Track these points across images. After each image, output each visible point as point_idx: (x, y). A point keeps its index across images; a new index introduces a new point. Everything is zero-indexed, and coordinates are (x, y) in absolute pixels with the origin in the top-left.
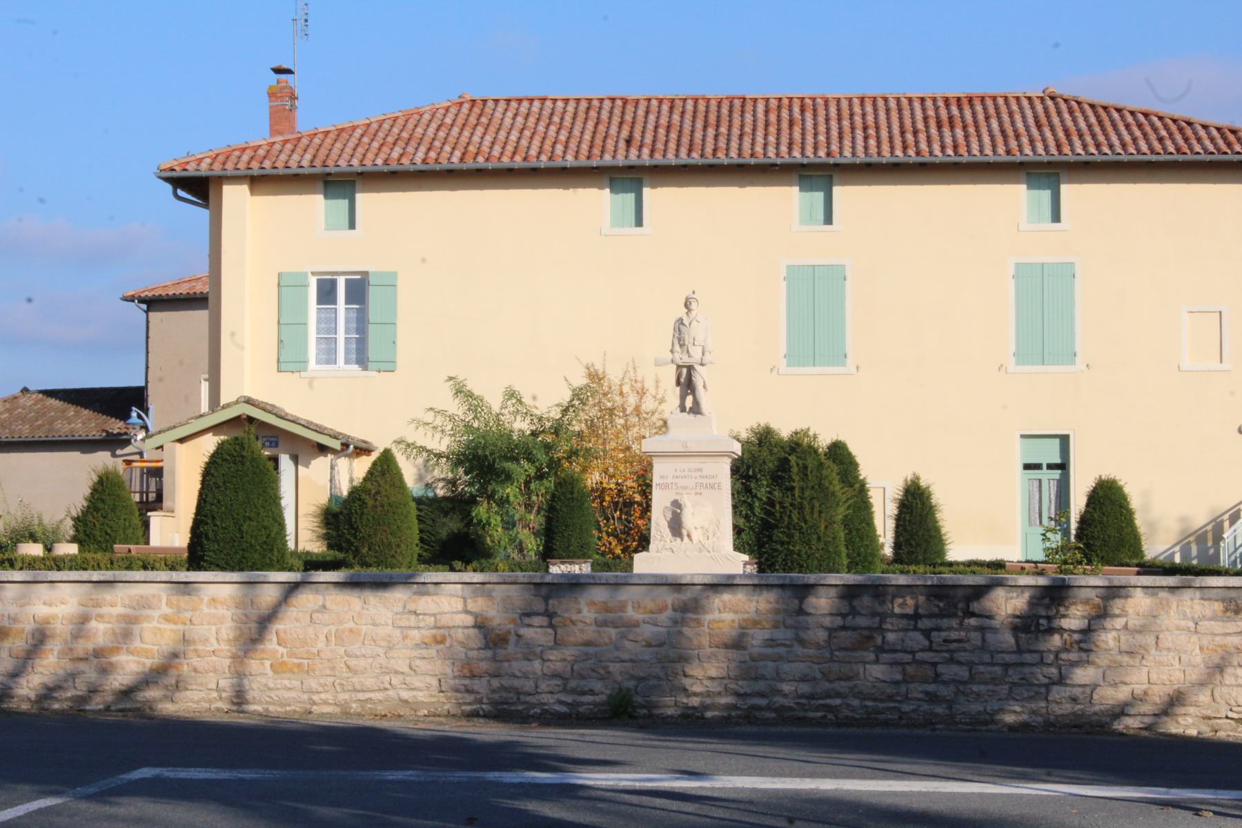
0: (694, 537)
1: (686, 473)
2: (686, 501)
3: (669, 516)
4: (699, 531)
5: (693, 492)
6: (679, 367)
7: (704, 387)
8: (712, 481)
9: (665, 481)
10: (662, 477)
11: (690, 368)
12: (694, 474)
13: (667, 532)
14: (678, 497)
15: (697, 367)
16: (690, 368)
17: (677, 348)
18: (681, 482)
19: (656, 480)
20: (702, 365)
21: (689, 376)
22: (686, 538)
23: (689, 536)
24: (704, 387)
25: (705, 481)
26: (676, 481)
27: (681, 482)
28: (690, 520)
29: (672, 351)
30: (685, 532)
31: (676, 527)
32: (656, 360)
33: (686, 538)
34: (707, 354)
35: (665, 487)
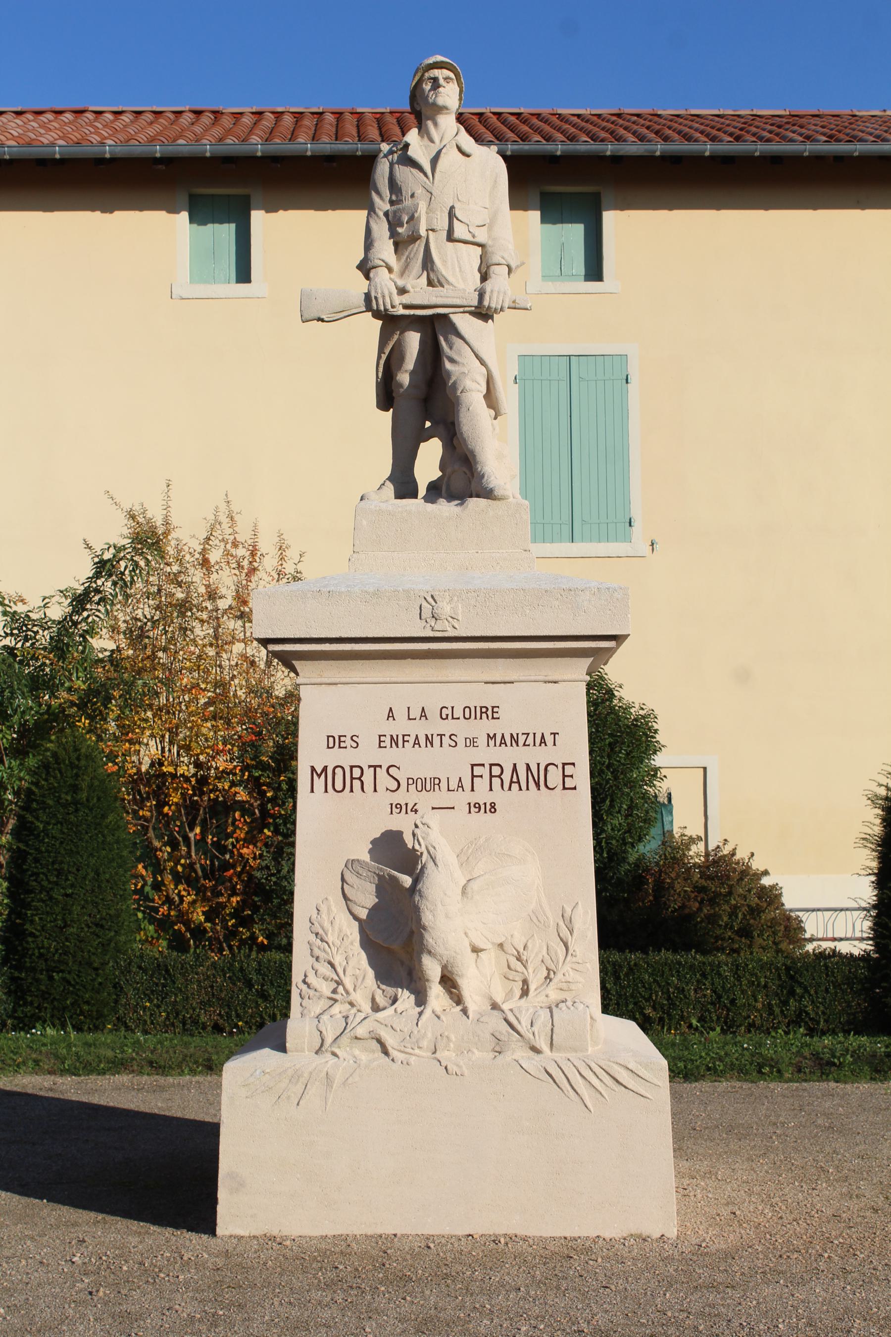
0: (469, 986)
1: (435, 726)
2: (440, 835)
3: (366, 898)
4: (489, 957)
5: (462, 799)
6: (392, 324)
7: (490, 398)
8: (537, 756)
9: (345, 757)
10: (335, 742)
11: (435, 327)
12: (463, 729)
13: (358, 965)
14: (402, 823)
15: (464, 323)
16: (435, 327)
17: (385, 249)
18: (413, 762)
19: (310, 753)
20: (483, 313)
21: (433, 358)
22: (436, 993)
23: (448, 981)
24: (490, 398)
25: (507, 756)
26: (388, 756)
27: (413, 762)
28: (453, 920)
29: (366, 268)
30: (432, 969)
31: (397, 944)
32: (305, 298)
33: (436, 993)
34: (499, 273)
35: (346, 780)
